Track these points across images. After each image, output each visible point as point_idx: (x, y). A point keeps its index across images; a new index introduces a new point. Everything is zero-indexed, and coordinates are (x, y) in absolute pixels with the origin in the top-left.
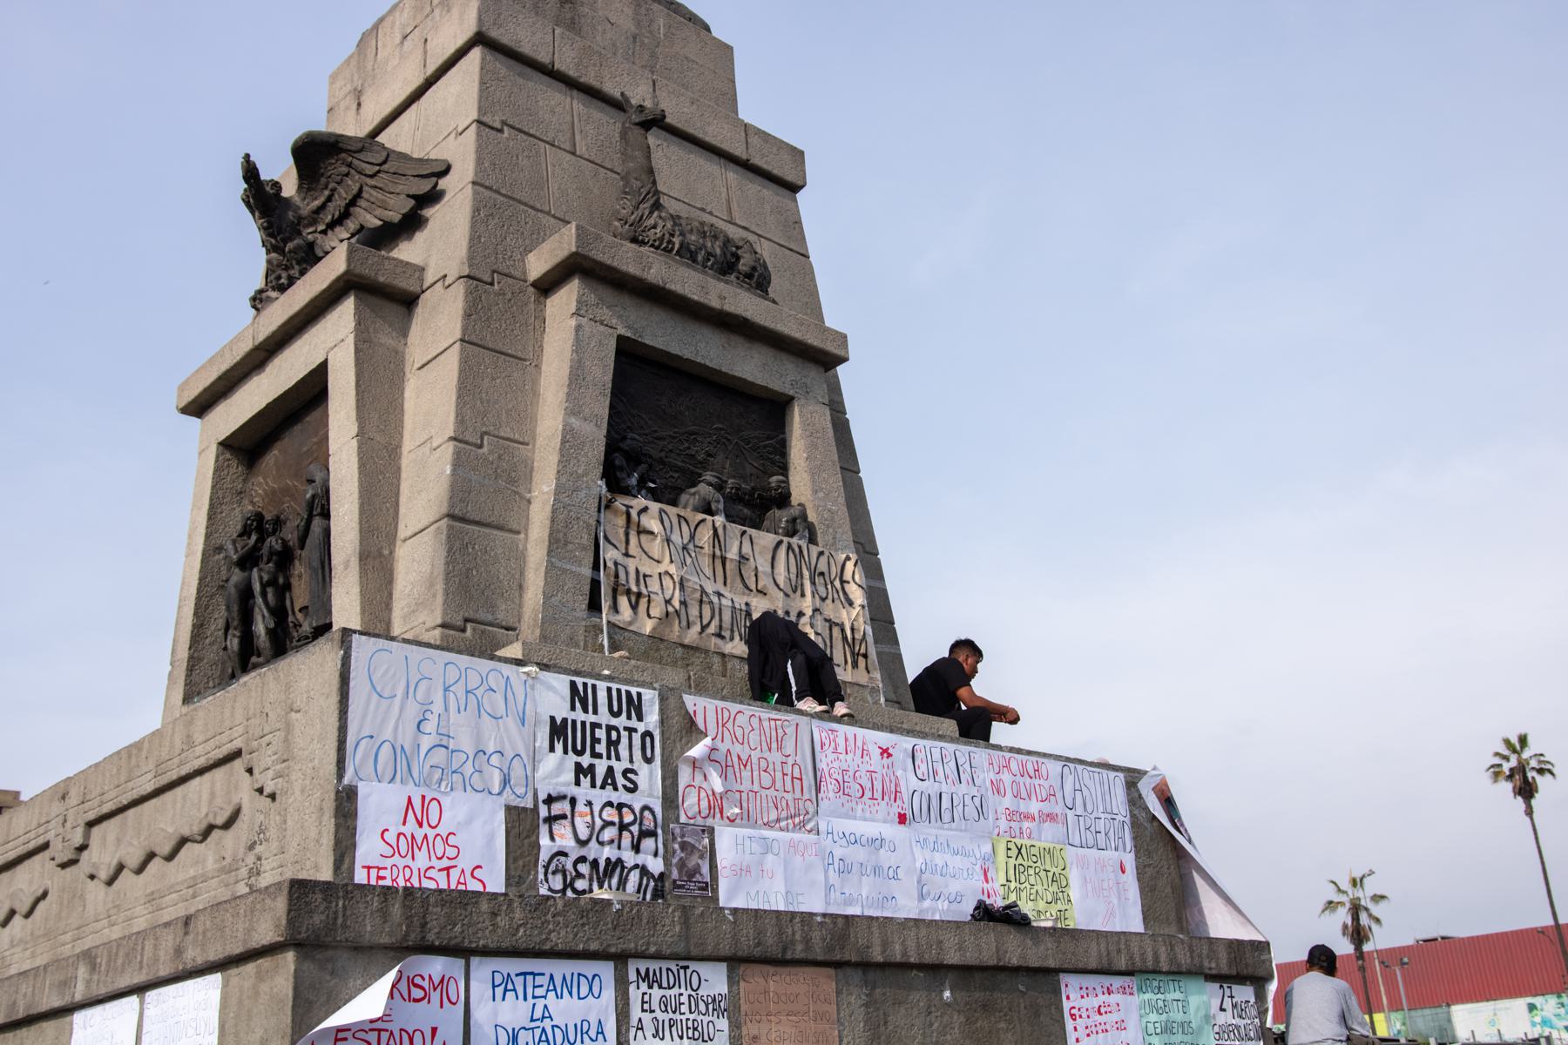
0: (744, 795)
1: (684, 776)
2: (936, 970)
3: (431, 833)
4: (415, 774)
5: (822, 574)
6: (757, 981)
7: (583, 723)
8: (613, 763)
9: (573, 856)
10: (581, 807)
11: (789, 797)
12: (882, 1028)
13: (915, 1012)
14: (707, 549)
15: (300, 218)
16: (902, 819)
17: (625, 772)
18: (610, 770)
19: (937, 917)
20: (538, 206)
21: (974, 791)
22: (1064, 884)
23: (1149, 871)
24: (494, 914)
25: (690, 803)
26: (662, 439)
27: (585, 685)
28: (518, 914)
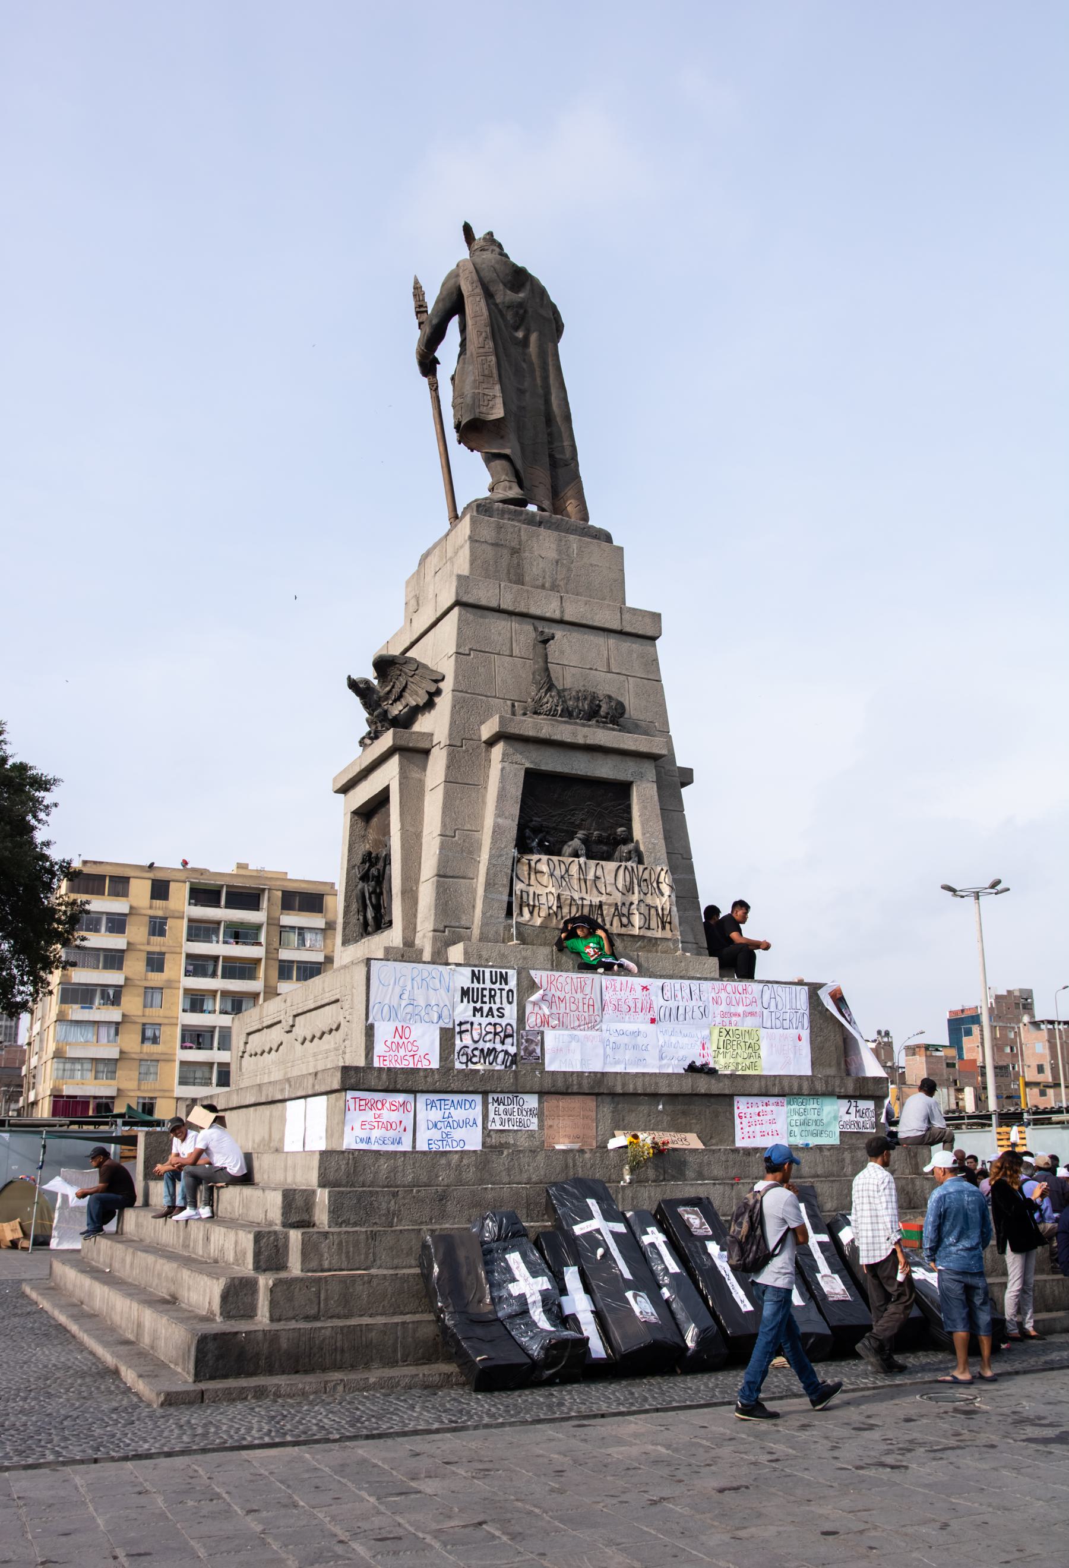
0: (561, 1016)
1: (529, 1008)
2: (655, 1096)
3: (406, 1041)
4: (399, 1016)
5: (646, 880)
6: (551, 1102)
7: (478, 989)
8: (492, 1005)
9: (471, 1048)
10: (476, 1026)
11: (586, 1014)
12: (621, 1123)
13: (641, 1115)
14: (576, 876)
15: (380, 698)
16: (653, 1021)
17: (498, 1010)
18: (491, 1009)
19: (670, 1071)
20: (489, 694)
21: (700, 1003)
22: (757, 1048)
23: (819, 1039)
24: (426, 1077)
25: (531, 1021)
26: (553, 816)
27: (479, 971)
28: (436, 1077)
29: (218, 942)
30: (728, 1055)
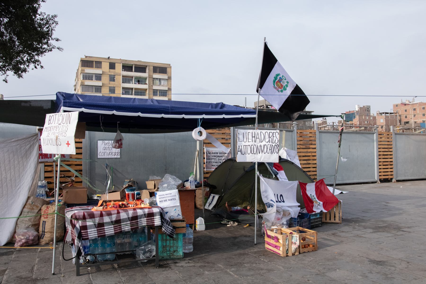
29: (132, 83)
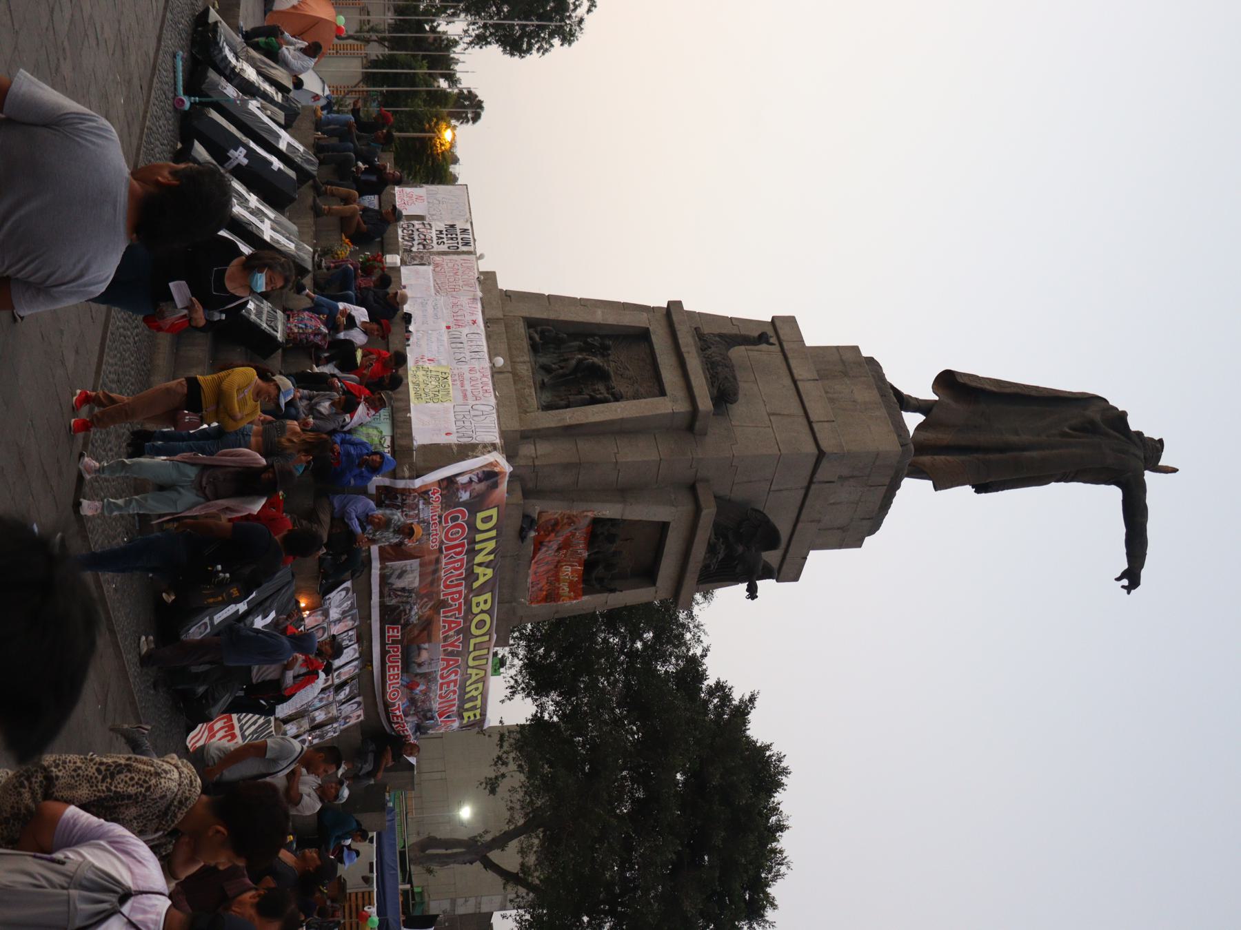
16: (448, 327)
25: (438, 259)
30: (425, 378)
